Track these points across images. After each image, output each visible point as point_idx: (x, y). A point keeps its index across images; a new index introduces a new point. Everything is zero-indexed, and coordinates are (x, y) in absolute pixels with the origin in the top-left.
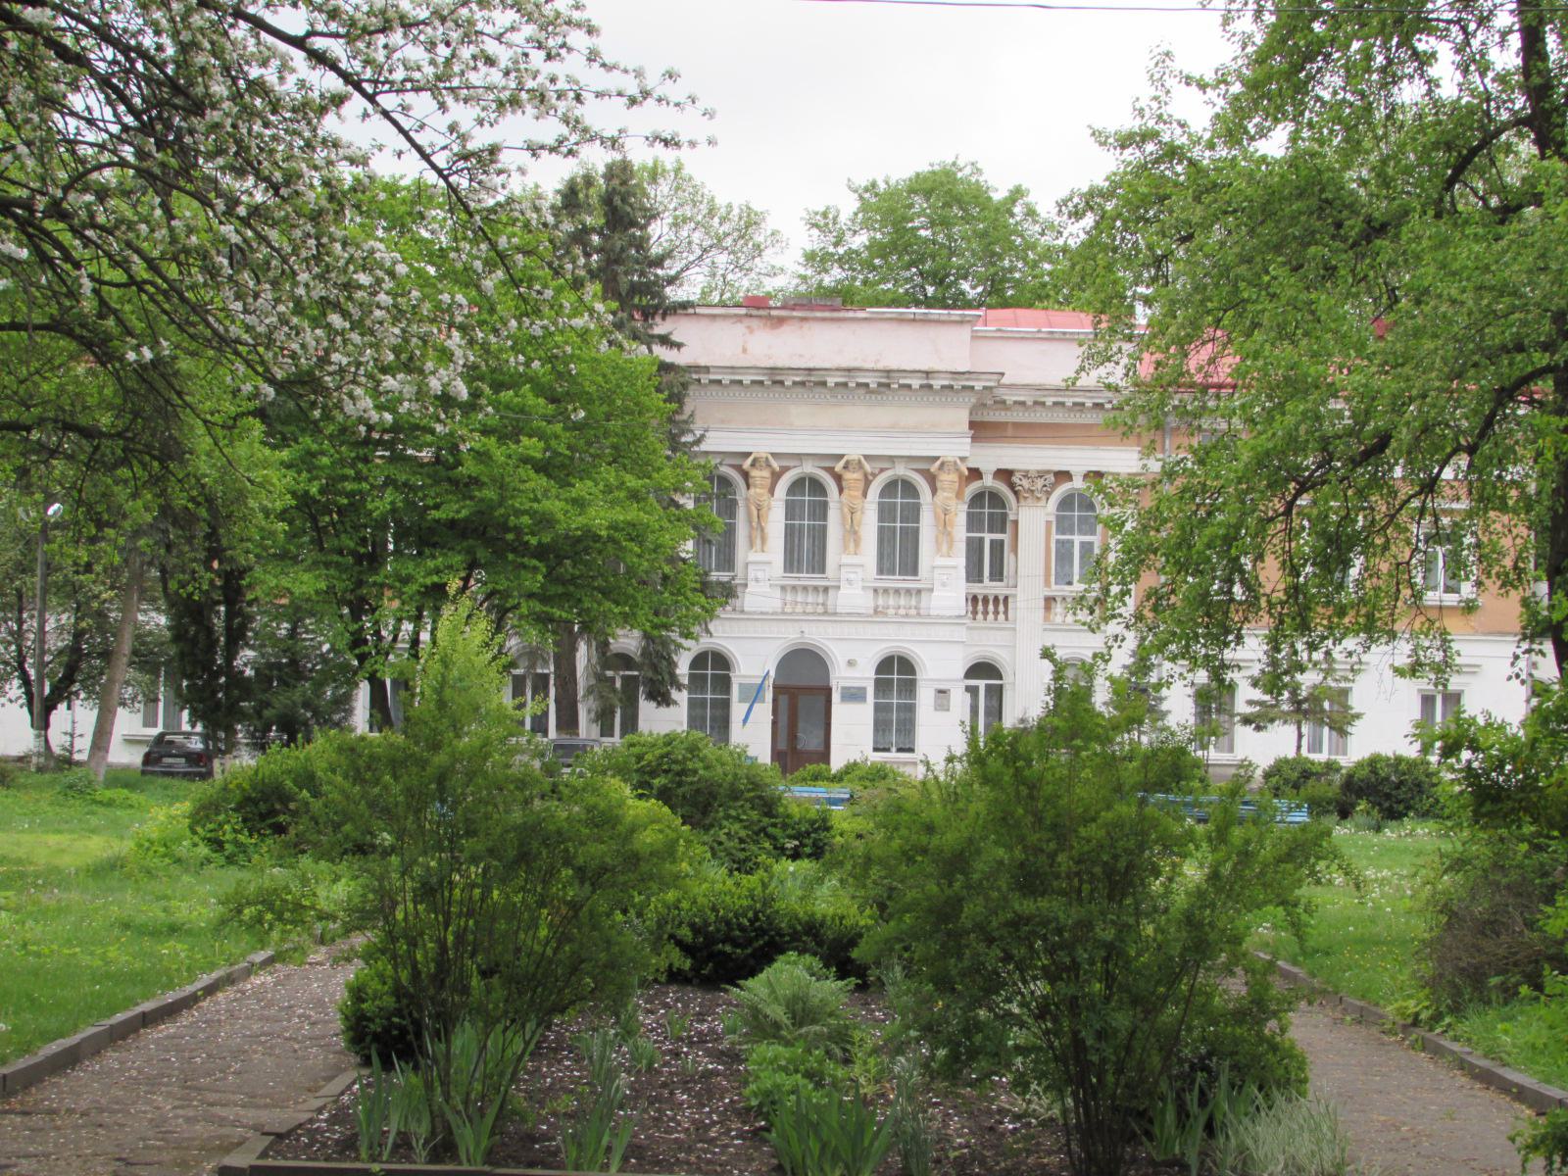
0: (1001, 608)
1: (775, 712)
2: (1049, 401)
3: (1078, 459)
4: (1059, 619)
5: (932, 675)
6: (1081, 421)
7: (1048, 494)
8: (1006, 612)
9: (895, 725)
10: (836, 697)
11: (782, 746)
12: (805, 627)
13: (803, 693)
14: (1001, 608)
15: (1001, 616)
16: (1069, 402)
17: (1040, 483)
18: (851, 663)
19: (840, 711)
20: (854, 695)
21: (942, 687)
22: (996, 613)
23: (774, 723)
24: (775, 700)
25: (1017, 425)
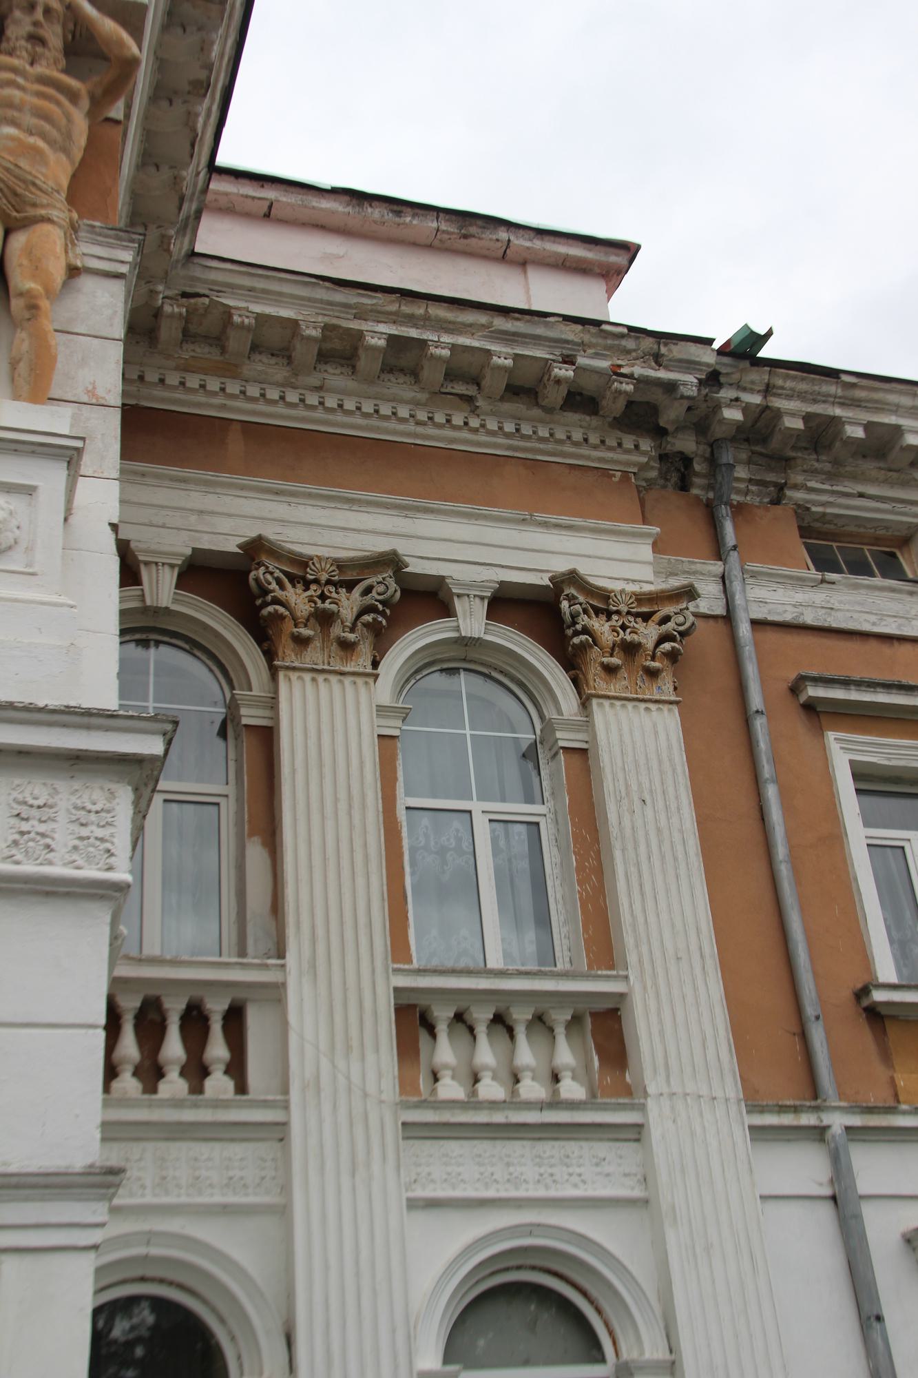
0: (217, 1050)
2: (377, 333)
3: (474, 547)
4: (450, 1089)
6: (463, 441)
7: (382, 639)
8: (237, 1068)
14: (217, 1050)
15: (219, 1084)
16: (441, 344)
17: (348, 604)
22: (197, 1071)
25: (256, 433)
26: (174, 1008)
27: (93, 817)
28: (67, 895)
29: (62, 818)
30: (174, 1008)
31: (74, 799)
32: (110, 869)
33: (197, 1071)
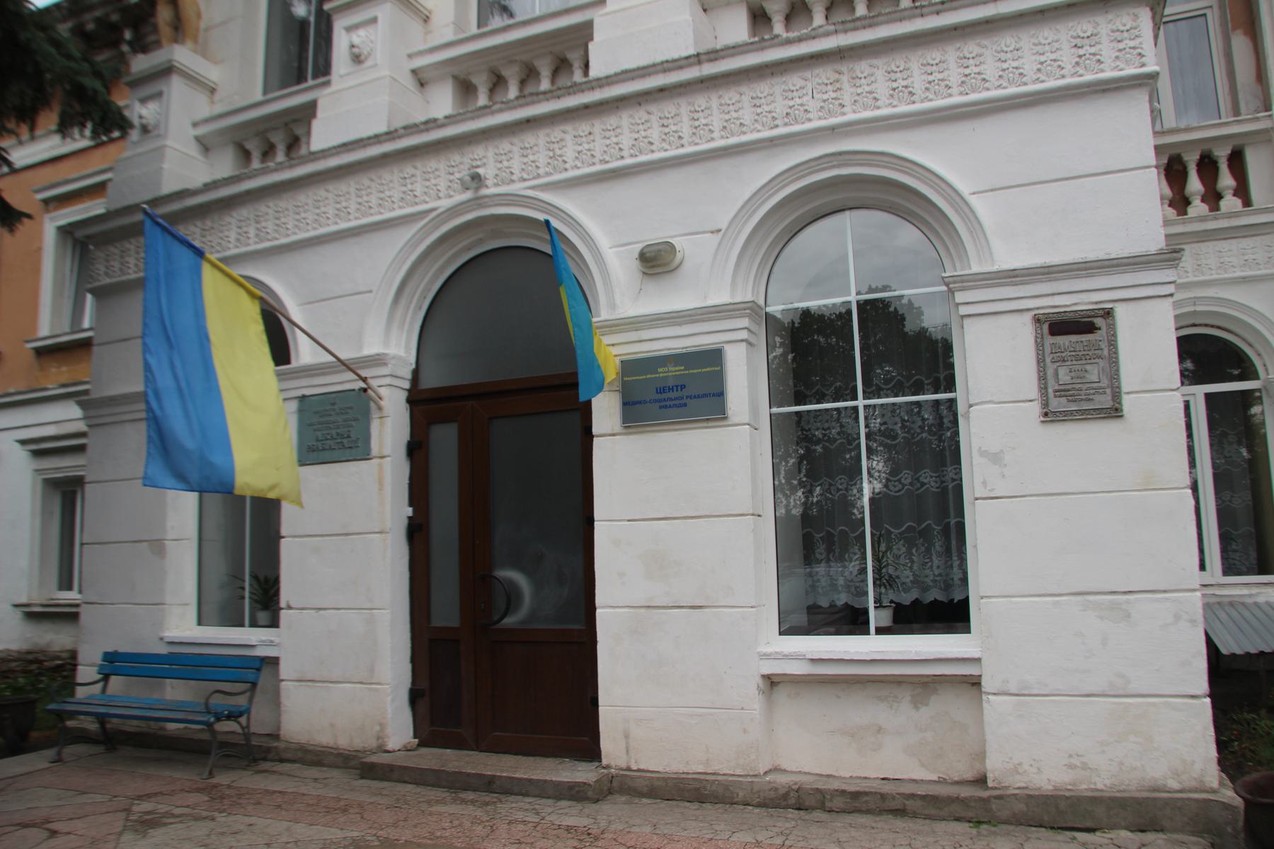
0: (1226, 181)
1: (419, 491)
5: (1007, 258)
8: (1242, 191)
9: (878, 526)
10: (605, 411)
11: (446, 614)
12: (488, 160)
13: (504, 427)
14: (1226, 181)
15: (1230, 203)
18: (656, 262)
19: (627, 469)
20: (677, 391)
21: (1072, 298)
23: (417, 532)
24: (417, 449)
26: (1191, 160)
27: (1126, 35)
28: (1117, 89)
29: (1105, 40)
30: (1191, 160)
31: (1110, 26)
32: (1143, 65)
33: (1213, 197)
